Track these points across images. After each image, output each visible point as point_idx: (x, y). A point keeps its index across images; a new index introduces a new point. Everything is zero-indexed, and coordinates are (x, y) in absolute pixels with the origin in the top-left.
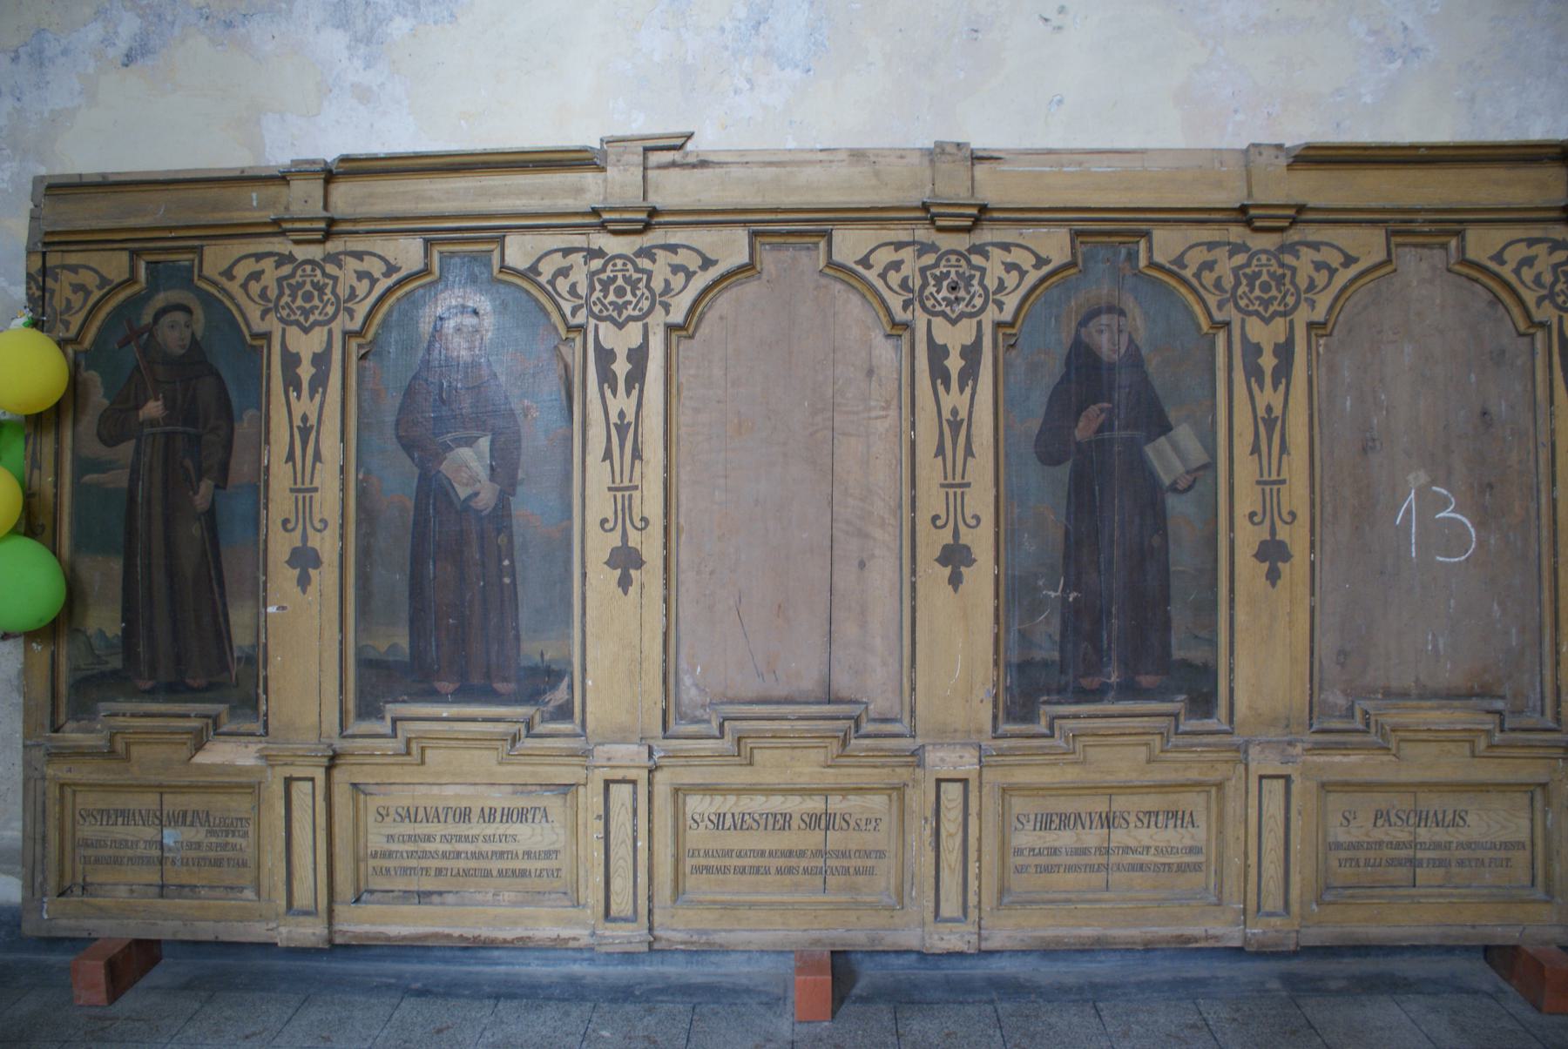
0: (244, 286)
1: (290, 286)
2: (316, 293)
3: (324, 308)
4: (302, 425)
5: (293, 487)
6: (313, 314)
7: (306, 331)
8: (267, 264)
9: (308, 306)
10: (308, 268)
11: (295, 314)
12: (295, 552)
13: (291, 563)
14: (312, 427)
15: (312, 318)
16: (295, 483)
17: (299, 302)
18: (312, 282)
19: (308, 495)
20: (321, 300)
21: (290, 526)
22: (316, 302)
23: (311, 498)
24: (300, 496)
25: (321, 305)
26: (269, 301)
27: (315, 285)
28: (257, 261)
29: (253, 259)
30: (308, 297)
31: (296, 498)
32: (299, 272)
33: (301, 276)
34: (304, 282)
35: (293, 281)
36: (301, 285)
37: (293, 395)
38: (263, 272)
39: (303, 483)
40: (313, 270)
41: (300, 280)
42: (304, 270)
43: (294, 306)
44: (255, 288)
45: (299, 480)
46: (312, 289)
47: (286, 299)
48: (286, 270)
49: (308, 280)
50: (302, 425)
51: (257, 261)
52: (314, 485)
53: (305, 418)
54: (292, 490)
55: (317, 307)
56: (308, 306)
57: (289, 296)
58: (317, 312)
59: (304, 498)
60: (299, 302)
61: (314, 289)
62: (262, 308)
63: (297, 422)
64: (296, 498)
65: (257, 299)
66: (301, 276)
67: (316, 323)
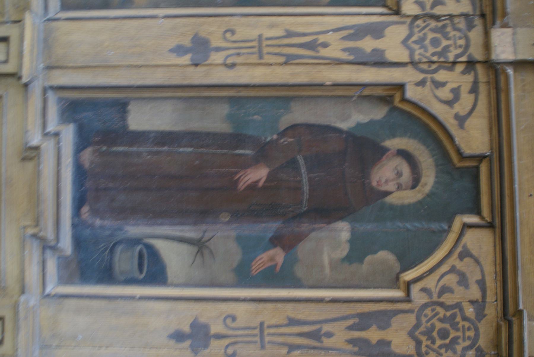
0: (453, 270)
1: (454, 316)
2: (447, 341)
3: (433, 350)
4: (323, 332)
5: (265, 325)
6: (427, 340)
7: (411, 334)
8: (475, 293)
9: (435, 334)
10: (471, 334)
11: (427, 322)
12: (206, 327)
13: (195, 325)
14: (322, 342)
15: (423, 338)
16: (269, 327)
17: (439, 325)
18: (458, 338)
19: (257, 339)
20: (441, 347)
21: (229, 321)
22: (439, 342)
23: (255, 342)
24: (257, 331)
25: (435, 347)
26: (439, 296)
27: (455, 341)
28: (478, 282)
29: (479, 277)
30: (444, 334)
31: (255, 328)
32: (467, 324)
33: (463, 326)
34: (457, 330)
35: (458, 319)
36: (455, 326)
37: (350, 322)
38: (467, 287)
39: (269, 334)
40: (469, 338)
41: (460, 325)
42: (469, 329)
43: (434, 320)
44: (451, 280)
45: (272, 331)
46: (451, 336)
47: (442, 312)
48: (470, 311)
49: (460, 334)
50: (323, 332)
51: (478, 282)
52: (267, 346)
53: (329, 335)
54: (262, 324)
55: (433, 342)
56: (435, 334)
57: (445, 315)
58: (429, 343)
59: (254, 336)
60: (439, 325)
61: (450, 341)
62: (433, 290)
63: (326, 328)
64: (255, 328)
65: (441, 283)
66: (463, 326)
67: (419, 343)
